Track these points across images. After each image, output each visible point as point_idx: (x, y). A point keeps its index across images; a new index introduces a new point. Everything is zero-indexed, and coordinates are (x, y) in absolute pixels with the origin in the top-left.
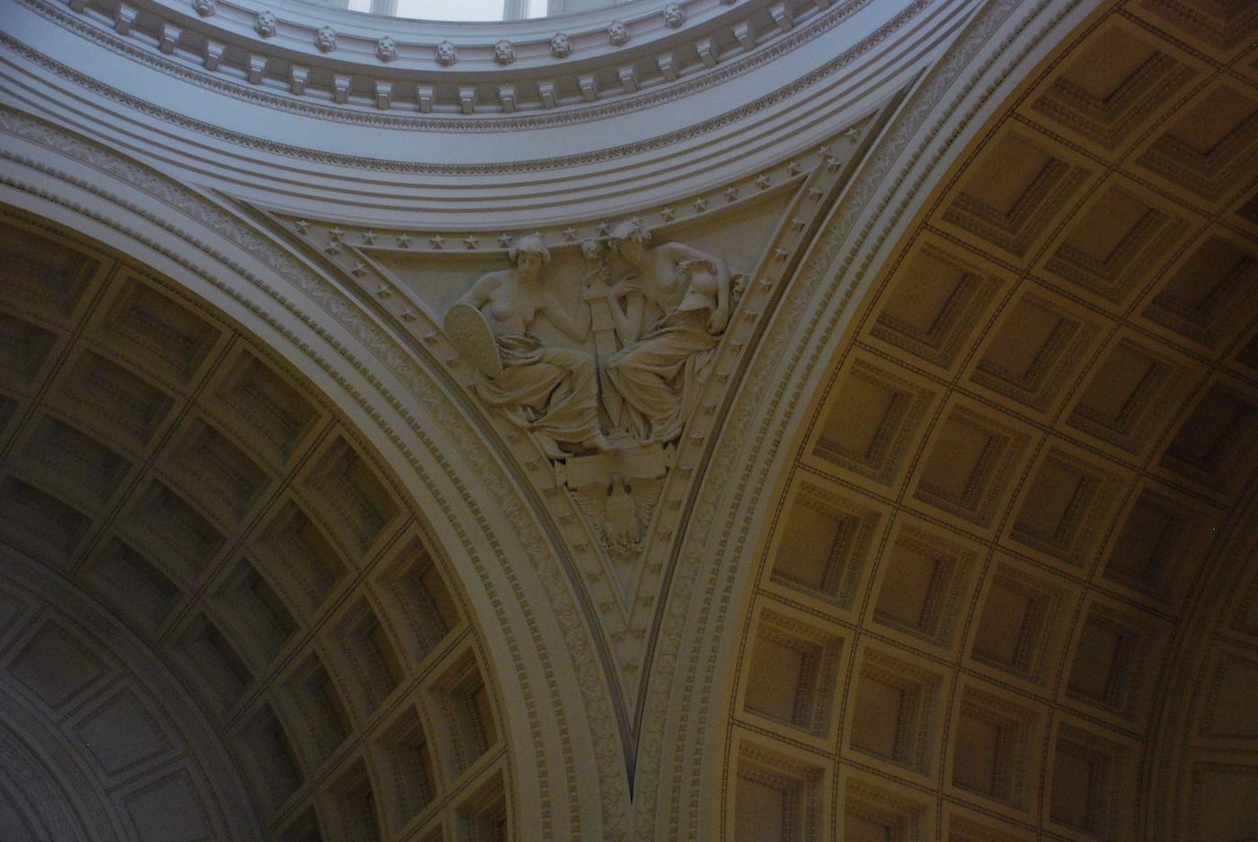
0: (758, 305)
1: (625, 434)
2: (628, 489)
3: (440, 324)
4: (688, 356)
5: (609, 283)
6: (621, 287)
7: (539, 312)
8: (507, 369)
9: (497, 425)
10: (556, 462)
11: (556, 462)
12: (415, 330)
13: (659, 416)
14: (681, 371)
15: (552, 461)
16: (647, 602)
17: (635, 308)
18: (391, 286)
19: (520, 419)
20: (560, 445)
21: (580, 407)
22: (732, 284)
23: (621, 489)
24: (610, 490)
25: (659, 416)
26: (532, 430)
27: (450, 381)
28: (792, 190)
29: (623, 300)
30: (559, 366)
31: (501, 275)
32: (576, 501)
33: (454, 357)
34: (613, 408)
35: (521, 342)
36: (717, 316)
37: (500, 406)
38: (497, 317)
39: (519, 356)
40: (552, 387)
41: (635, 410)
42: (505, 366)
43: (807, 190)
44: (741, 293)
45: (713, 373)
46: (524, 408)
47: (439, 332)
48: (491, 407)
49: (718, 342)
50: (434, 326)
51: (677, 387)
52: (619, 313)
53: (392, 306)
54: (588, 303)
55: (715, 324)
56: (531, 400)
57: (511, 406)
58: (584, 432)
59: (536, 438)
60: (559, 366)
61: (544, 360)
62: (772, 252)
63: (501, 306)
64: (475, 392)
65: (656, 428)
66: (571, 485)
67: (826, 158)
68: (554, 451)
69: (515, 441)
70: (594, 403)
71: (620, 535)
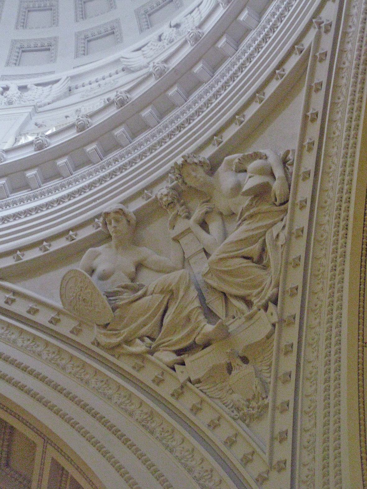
0: (309, 162)
1: (232, 320)
2: (245, 360)
3: (58, 304)
4: (265, 232)
5: (188, 217)
6: (198, 212)
7: (139, 266)
8: (118, 310)
9: (126, 365)
10: (177, 367)
11: (177, 367)
12: (43, 318)
13: (255, 291)
14: (263, 249)
15: (174, 369)
16: (282, 438)
17: (215, 226)
18: (15, 293)
19: (139, 347)
20: (179, 353)
21: (185, 313)
22: (285, 162)
23: (239, 361)
24: (230, 369)
25: (255, 291)
26: (152, 353)
27: (80, 347)
28: (302, 65)
29: (204, 225)
30: (162, 292)
31: (100, 249)
32: (201, 390)
33: (73, 324)
34: (218, 307)
35: (126, 287)
36: (277, 186)
37: (119, 345)
38: (104, 277)
39: (127, 296)
40: (162, 310)
41: (236, 297)
42: (114, 309)
43: (315, 57)
44: (292, 164)
45: (290, 233)
46: (141, 338)
47: (59, 312)
48: (111, 349)
49: (286, 211)
50: (53, 308)
51: (265, 262)
52: (203, 233)
53: (20, 307)
54: (176, 239)
55: (278, 193)
56: (144, 330)
57: (128, 342)
58: (193, 331)
59: (158, 358)
60: (162, 292)
61: (149, 293)
62: (305, 117)
63: (102, 266)
64: (98, 344)
65: (255, 301)
66: (192, 379)
67: (319, 24)
68: (173, 357)
69: (139, 368)
70: (197, 304)
71: (248, 400)
